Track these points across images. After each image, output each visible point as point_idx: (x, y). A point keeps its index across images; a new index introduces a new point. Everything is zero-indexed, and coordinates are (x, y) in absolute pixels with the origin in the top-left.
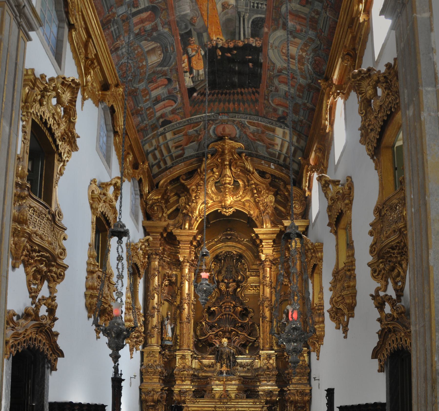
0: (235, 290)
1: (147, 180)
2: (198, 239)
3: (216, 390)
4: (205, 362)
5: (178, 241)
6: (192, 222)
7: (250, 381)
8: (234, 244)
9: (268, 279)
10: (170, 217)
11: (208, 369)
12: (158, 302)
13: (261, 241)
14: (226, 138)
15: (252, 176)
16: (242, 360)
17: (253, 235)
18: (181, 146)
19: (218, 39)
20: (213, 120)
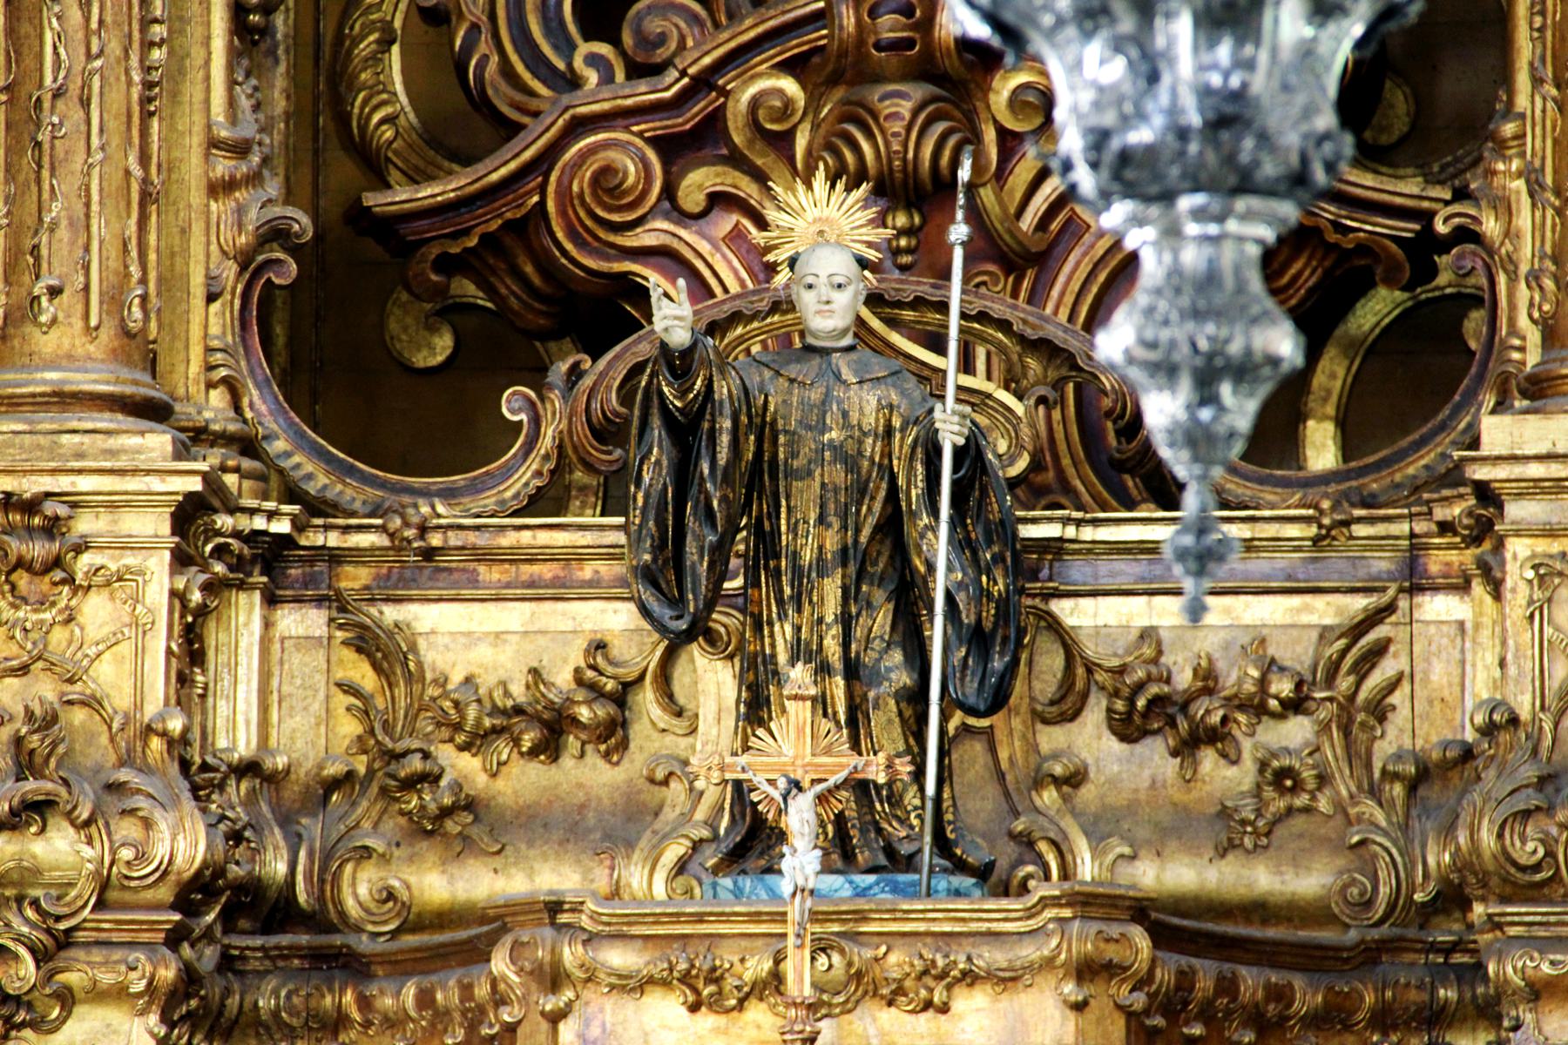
4: (475, 640)
7: (1307, 996)
11: (519, 780)
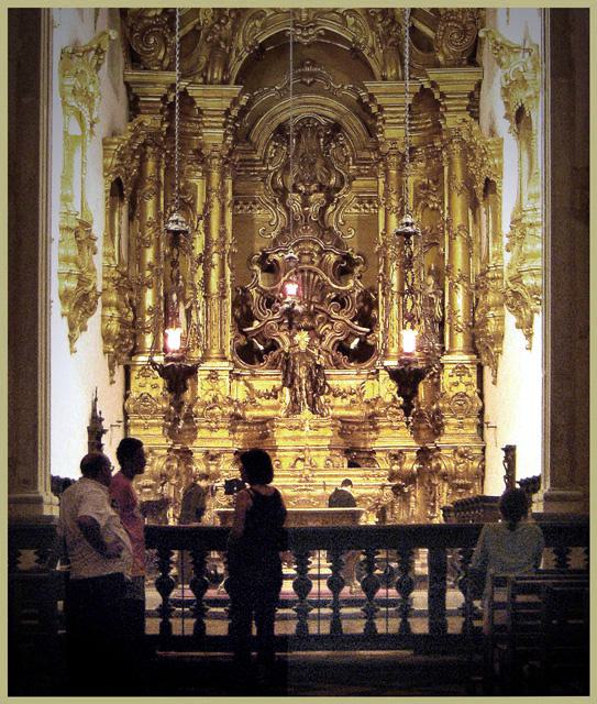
0: (323, 209)
5: (199, 108)
7: (356, 428)
11: (264, 402)
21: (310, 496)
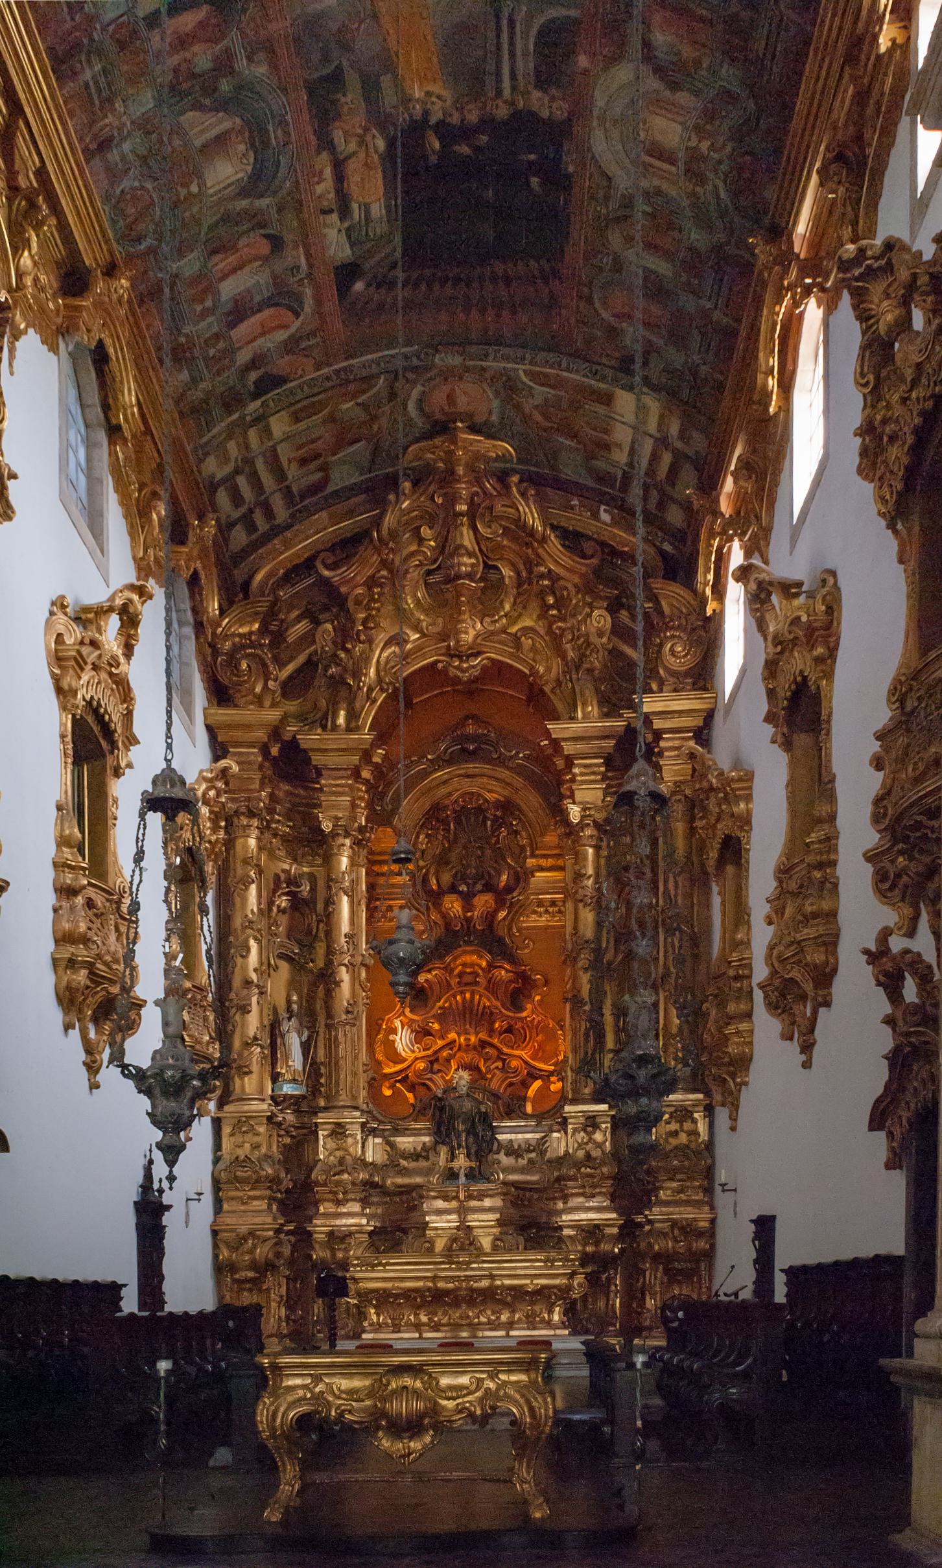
1: (214, 570)
2: (376, 760)
3: (436, 1229)
5: (316, 767)
6: (358, 705)
8: (486, 768)
9: (590, 882)
10: (289, 688)
11: (413, 1165)
12: (261, 964)
13: (569, 762)
14: (460, 425)
15: (540, 551)
16: (513, 1133)
17: (546, 742)
18: (317, 456)
19: (428, 94)
20: (414, 369)
21: (472, 1290)
